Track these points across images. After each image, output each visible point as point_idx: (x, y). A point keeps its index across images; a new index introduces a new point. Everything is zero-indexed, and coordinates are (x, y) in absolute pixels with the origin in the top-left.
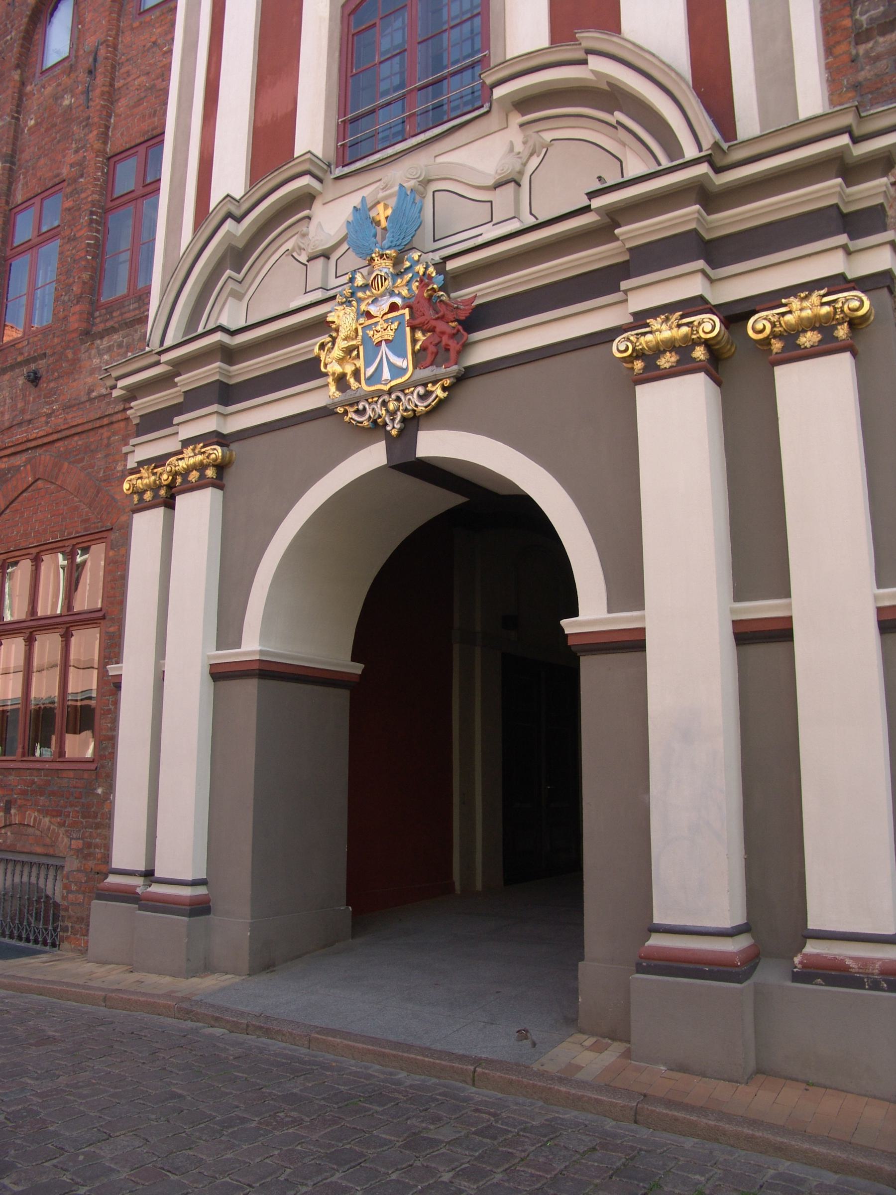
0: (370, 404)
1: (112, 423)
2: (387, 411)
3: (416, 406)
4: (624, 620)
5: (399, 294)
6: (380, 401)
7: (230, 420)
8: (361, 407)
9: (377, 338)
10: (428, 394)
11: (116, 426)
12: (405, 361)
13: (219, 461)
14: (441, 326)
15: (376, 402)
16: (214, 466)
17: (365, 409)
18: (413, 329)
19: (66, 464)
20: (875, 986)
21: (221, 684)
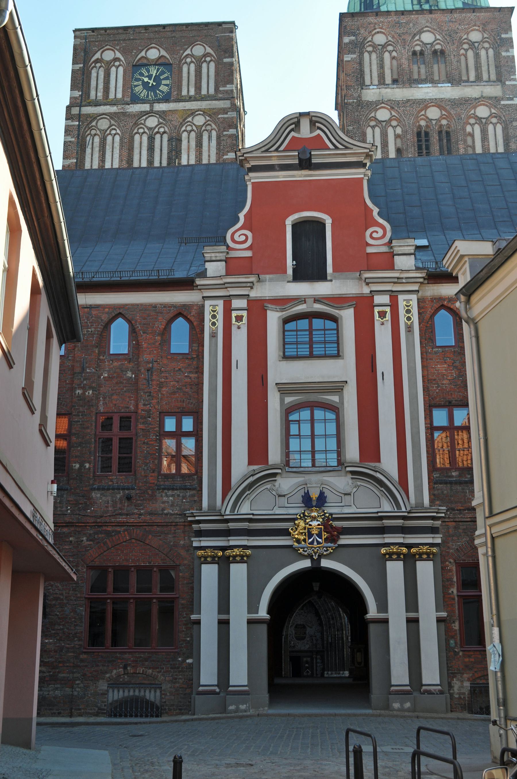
1: (177, 525)
4: (382, 615)
9: (313, 532)
10: (327, 550)
11: (178, 527)
19: (150, 536)
20: (437, 694)
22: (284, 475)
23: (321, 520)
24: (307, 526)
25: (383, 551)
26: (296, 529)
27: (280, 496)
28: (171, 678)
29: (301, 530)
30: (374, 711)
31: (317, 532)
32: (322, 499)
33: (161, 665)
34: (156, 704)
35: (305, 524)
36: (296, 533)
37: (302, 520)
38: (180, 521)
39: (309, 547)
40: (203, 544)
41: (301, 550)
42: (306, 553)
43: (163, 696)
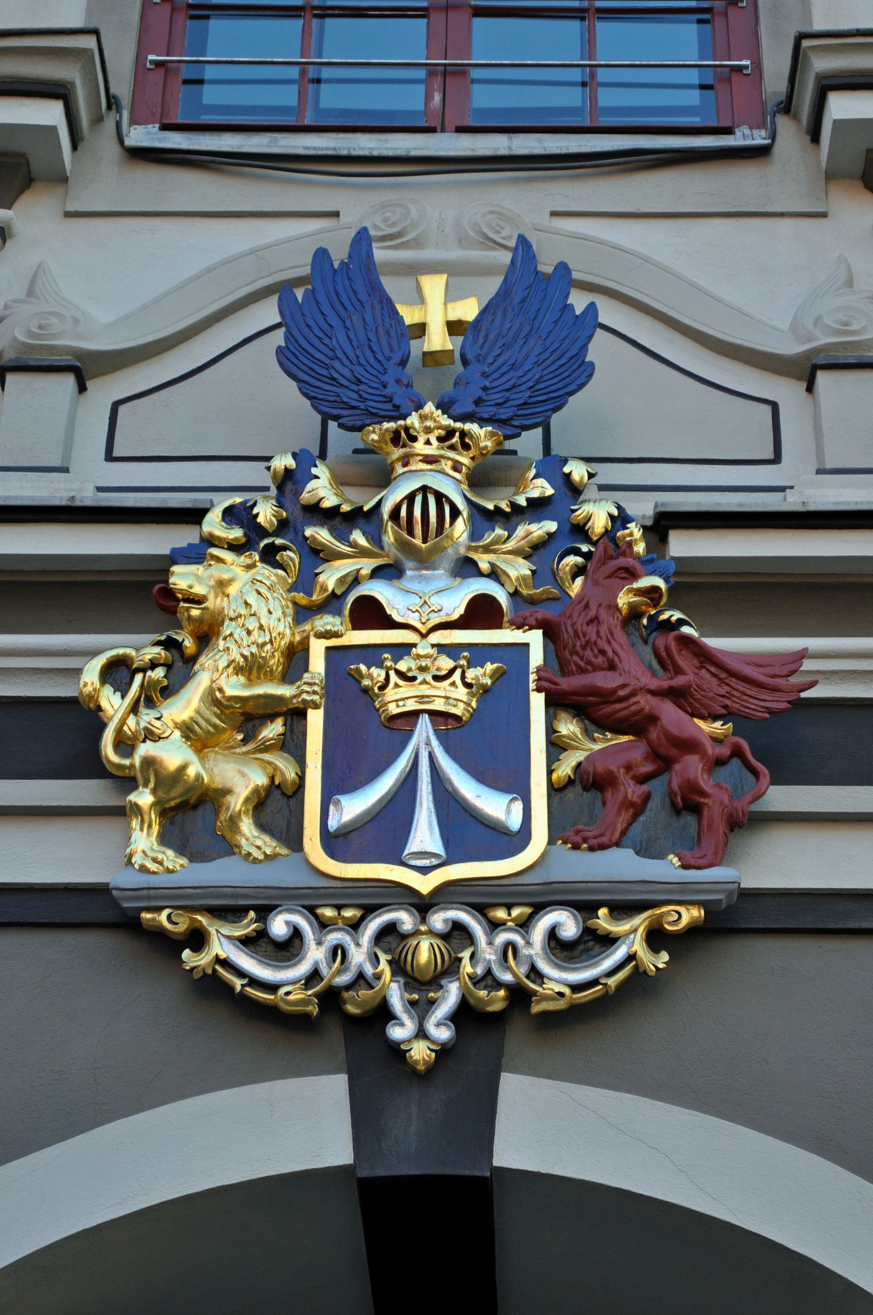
0: (323, 925)
2: (398, 967)
3: (535, 973)
5: (494, 574)
9: (398, 698)
12: (518, 806)
15: (355, 926)
17: (296, 933)
18: (556, 703)
22: (104, 179)
23: (519, 569)
24: (327, 622)
26: (181, 665)
31: (455, 697)
32: (533, 349)
35: (303, 613)
37: (270, 556)
41: (223, 942)
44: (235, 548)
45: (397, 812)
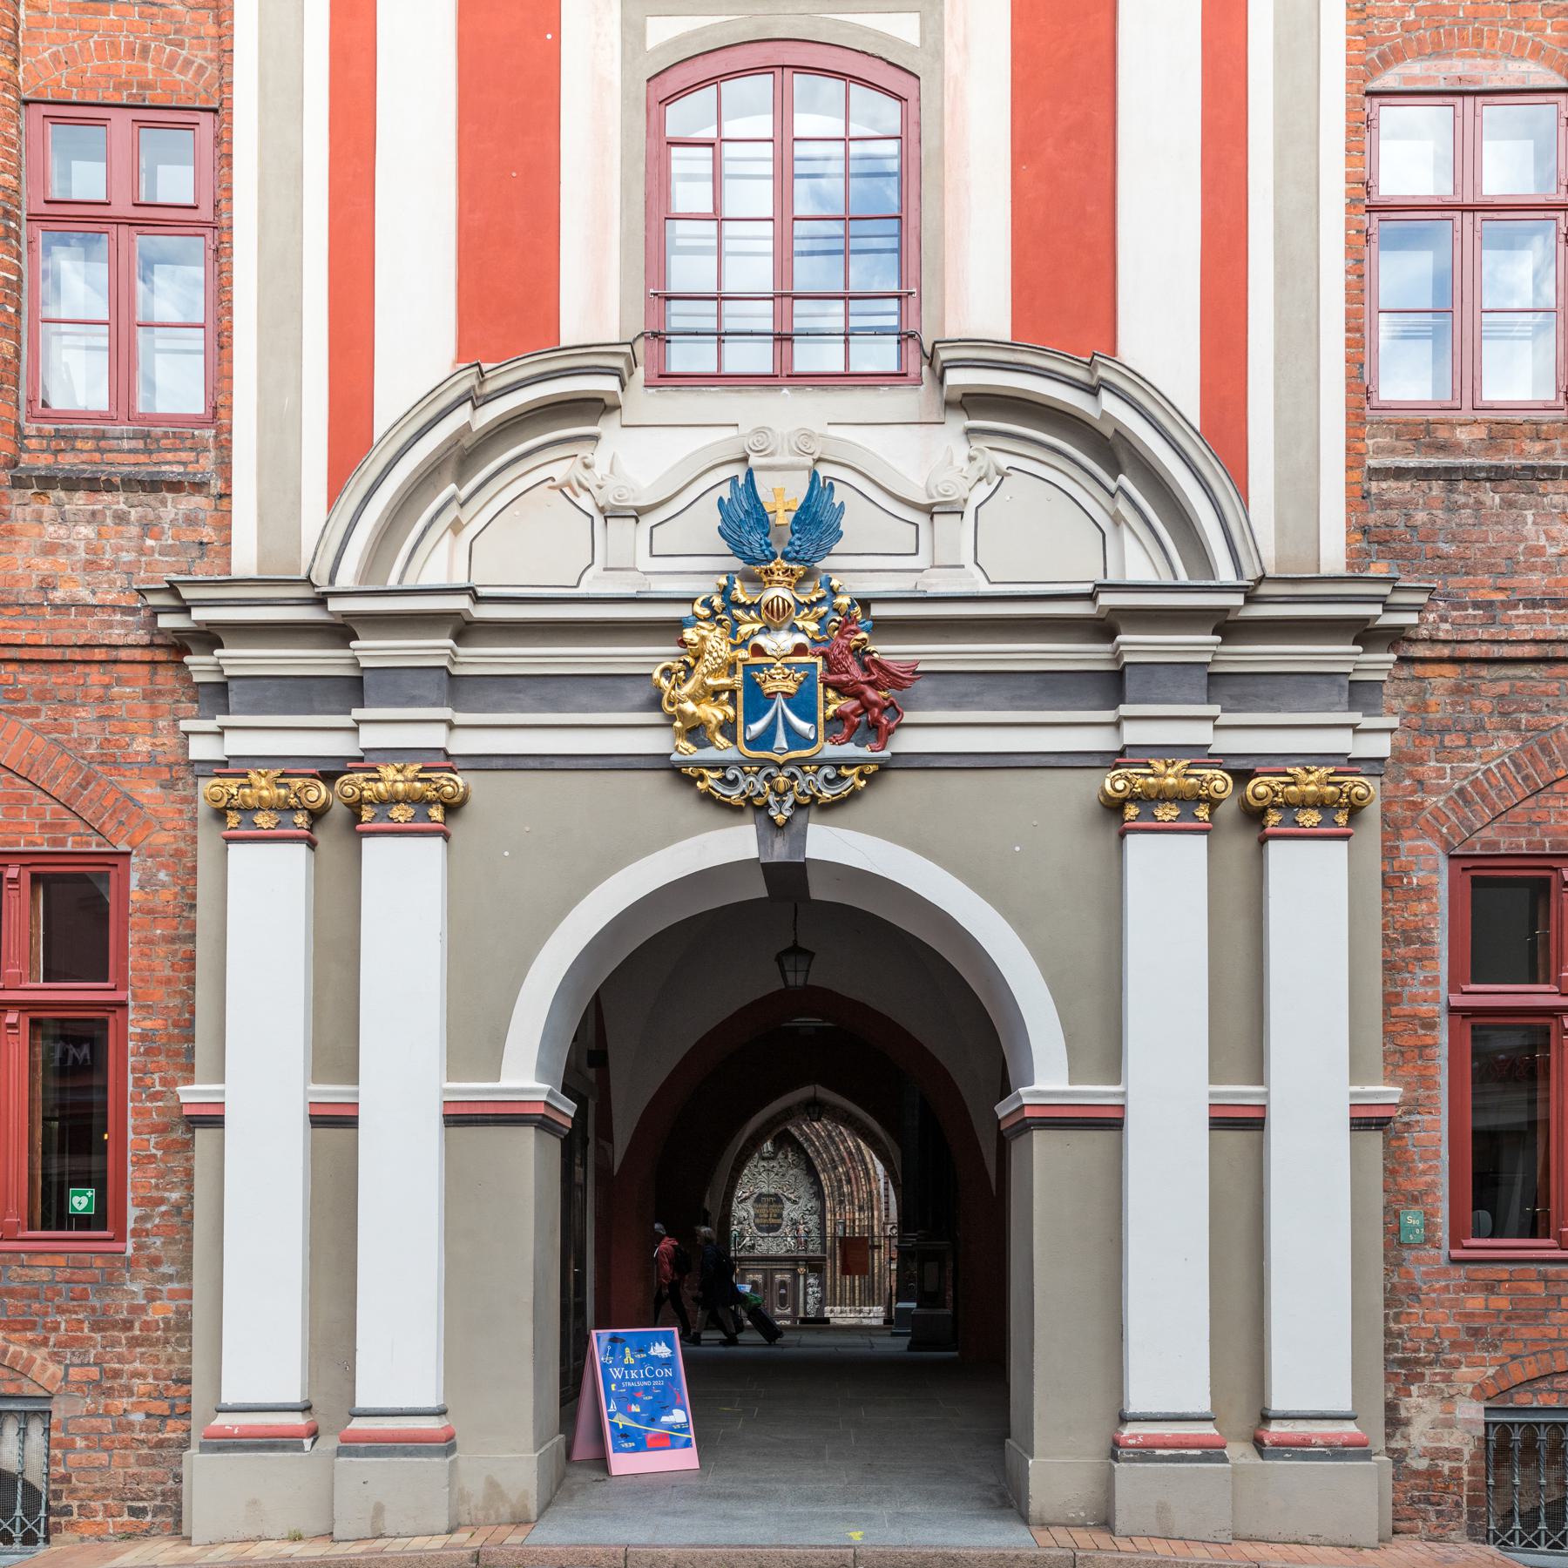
2: (772, 788)
3: (819, 791)
5: (804, 631)
6: (763, 774)
7: (458, 733)
8: (730, 777)
13: (456, 799)
14: (871, 694)
15: (757, 773)
16: (443, 804)
18: (827, 685)
21: (457, 1131)
25: (1114, 783)
26: (689, 670)
27: (610, 514)
28: (94, 1372)
29: (713, 673)
30: (1044, 1537)
31: (791, 687)
33: (46, 1314)
34: (26, 1484)
35: (734, 647)
36: (688, 688)
38: (130, 640)
39: (751, 761)
40: (237, 744)
42: (734, 795)
43: (57, 1453)
44: (705, 620)
45: (770, 732)
